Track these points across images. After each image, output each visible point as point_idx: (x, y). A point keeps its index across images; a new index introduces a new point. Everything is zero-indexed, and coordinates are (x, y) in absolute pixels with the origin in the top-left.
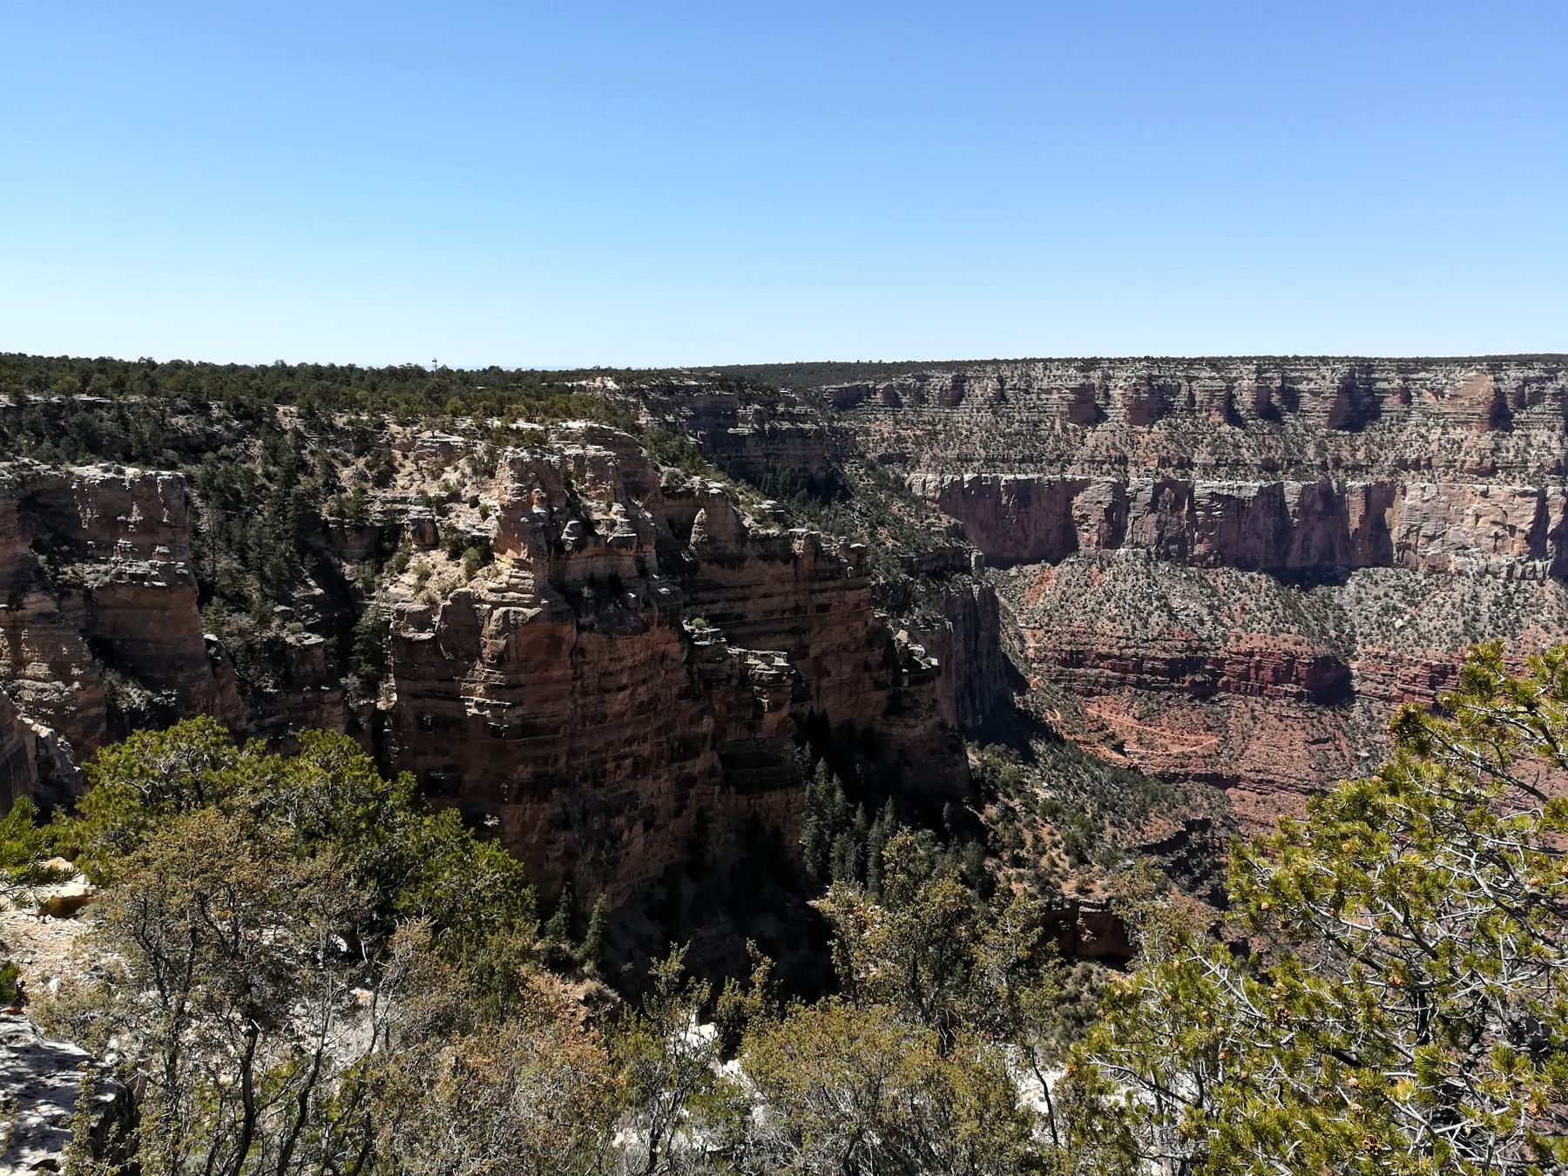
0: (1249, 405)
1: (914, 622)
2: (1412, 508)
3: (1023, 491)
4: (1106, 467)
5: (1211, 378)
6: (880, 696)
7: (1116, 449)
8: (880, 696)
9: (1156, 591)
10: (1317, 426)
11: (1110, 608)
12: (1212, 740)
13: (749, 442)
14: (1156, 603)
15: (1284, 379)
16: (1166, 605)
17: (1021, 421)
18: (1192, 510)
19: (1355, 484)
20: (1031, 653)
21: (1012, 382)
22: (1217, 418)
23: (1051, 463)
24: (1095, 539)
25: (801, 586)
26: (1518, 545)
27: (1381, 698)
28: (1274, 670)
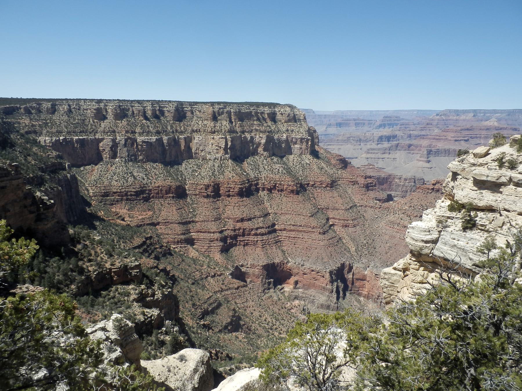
0: (150, 114)
1: (46, 189)
2: (197, 143)
3: (82, 142)
4: (109, 134)
5: (139, 106)
6: (32, 216)
7: (111, 128)
10: (170, 121)
12: (150, 213)
15: (159, 107)
16: (133, 175)
17: (78, 119)
18: (137, 146)
20: (91, 194)
21: (73, 106)
22: (141, 118)
23: (90, 133)
24: (108, 156)
26: (222, 151)
27: (194, 195)
28: (166, 191)
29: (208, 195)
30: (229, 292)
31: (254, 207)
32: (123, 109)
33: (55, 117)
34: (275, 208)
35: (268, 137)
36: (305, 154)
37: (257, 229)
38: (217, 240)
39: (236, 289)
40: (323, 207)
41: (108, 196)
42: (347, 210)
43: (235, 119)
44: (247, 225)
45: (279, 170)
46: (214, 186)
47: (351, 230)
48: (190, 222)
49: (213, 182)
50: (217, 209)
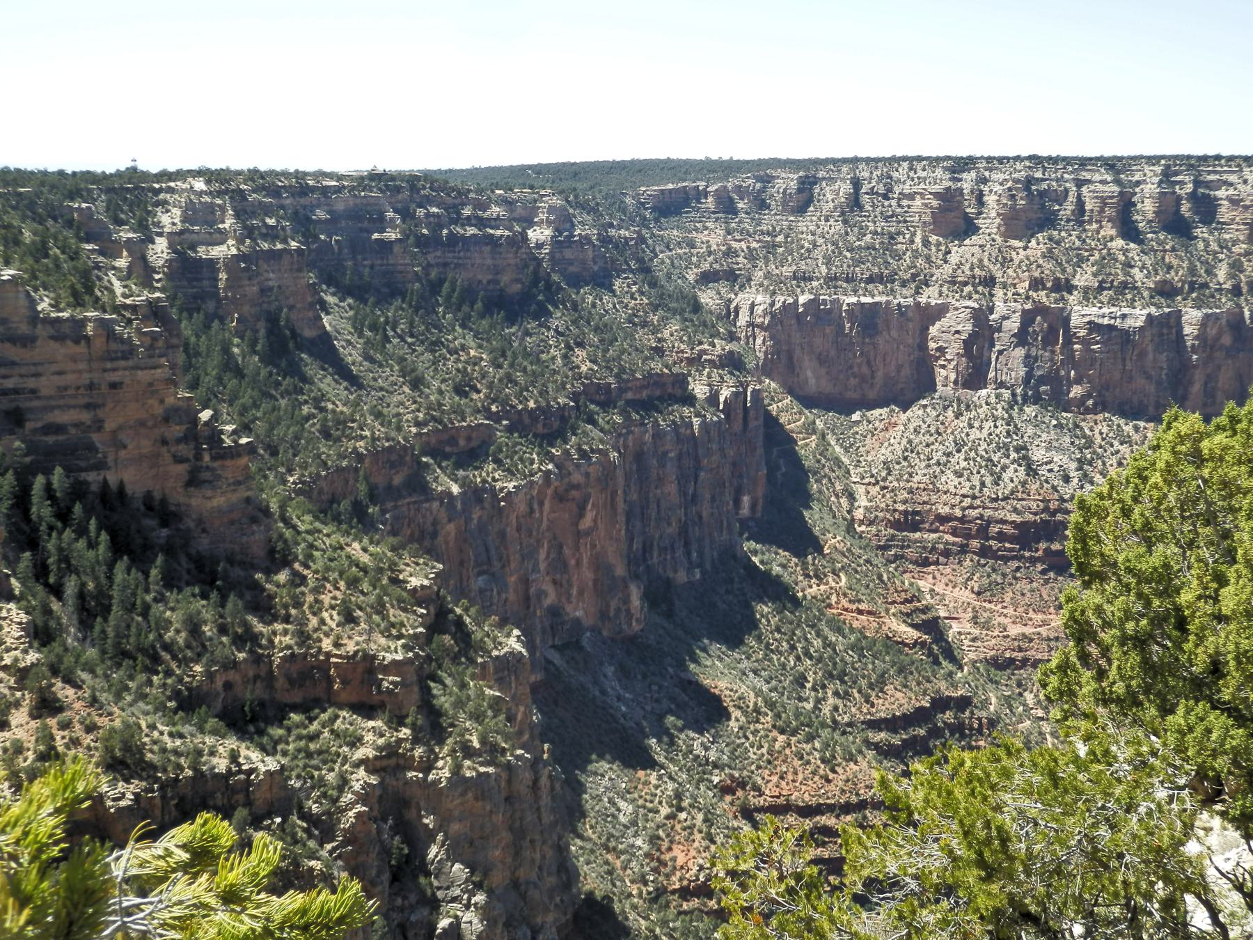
0: (1150, 216)
1: (567, 452)
3: (869, 317)
4: (969, 288)
5: (1103, 182)
6: (182, 469)
7: (981, 267)
8: (182, 469)
9: (1016, 441)
10: (1235, 242)
11: (959, 461)
13: (396, 249)
14: (1013, 455)
15: (1197, 183)
16: (1025, 458)
17: (876, 233)
18: (1068, 342)
22: (1109, 230)
23: (904, 284)
24: (953, 376)
25: (95, 365)
32: (1042, 194)
33: (805, 224)
41: (915, 528)
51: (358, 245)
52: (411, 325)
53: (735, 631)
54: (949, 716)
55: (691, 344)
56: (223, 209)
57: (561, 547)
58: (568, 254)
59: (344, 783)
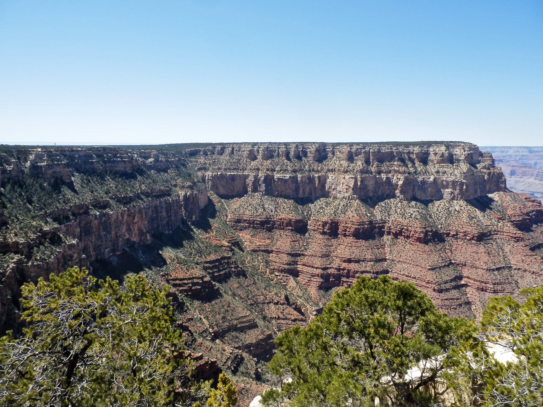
2: (330, 182)
3: (233, 178)
11: (250, 208)
12: (268, 241)
15: (303, 148)
19: (316, 175)
20: (228, 220)
22: (284, 158)
23: (241, 170)
26: (351, 191)
27: (313, 230)
29: (324, 232)
30: (285, 322)
31: (368, 250)
32: (270, 151)
33: (222, 157)
34: (394, 255)
35: (406, 178)
36: (457, 200)
37: (362, 272)
38: (318, 275)
39: (292, 321)
40: (458, 262)
41: (240, 222)
42: (489, 270)
43: (373, 159)
44: (353, 267)
45: (412, 214)
46: (331, 224)
47: (488, 295)
48: (299, 255)
49: (331, 220)
50: (330, 246)
51: (86, 163)
52: (97, 179)
53: (177, 245)
54: (226, 261)
55: (182, 183)
56: (44, 155)
57: (129, 226)
58: (157, 164)
59: (8, 266)
